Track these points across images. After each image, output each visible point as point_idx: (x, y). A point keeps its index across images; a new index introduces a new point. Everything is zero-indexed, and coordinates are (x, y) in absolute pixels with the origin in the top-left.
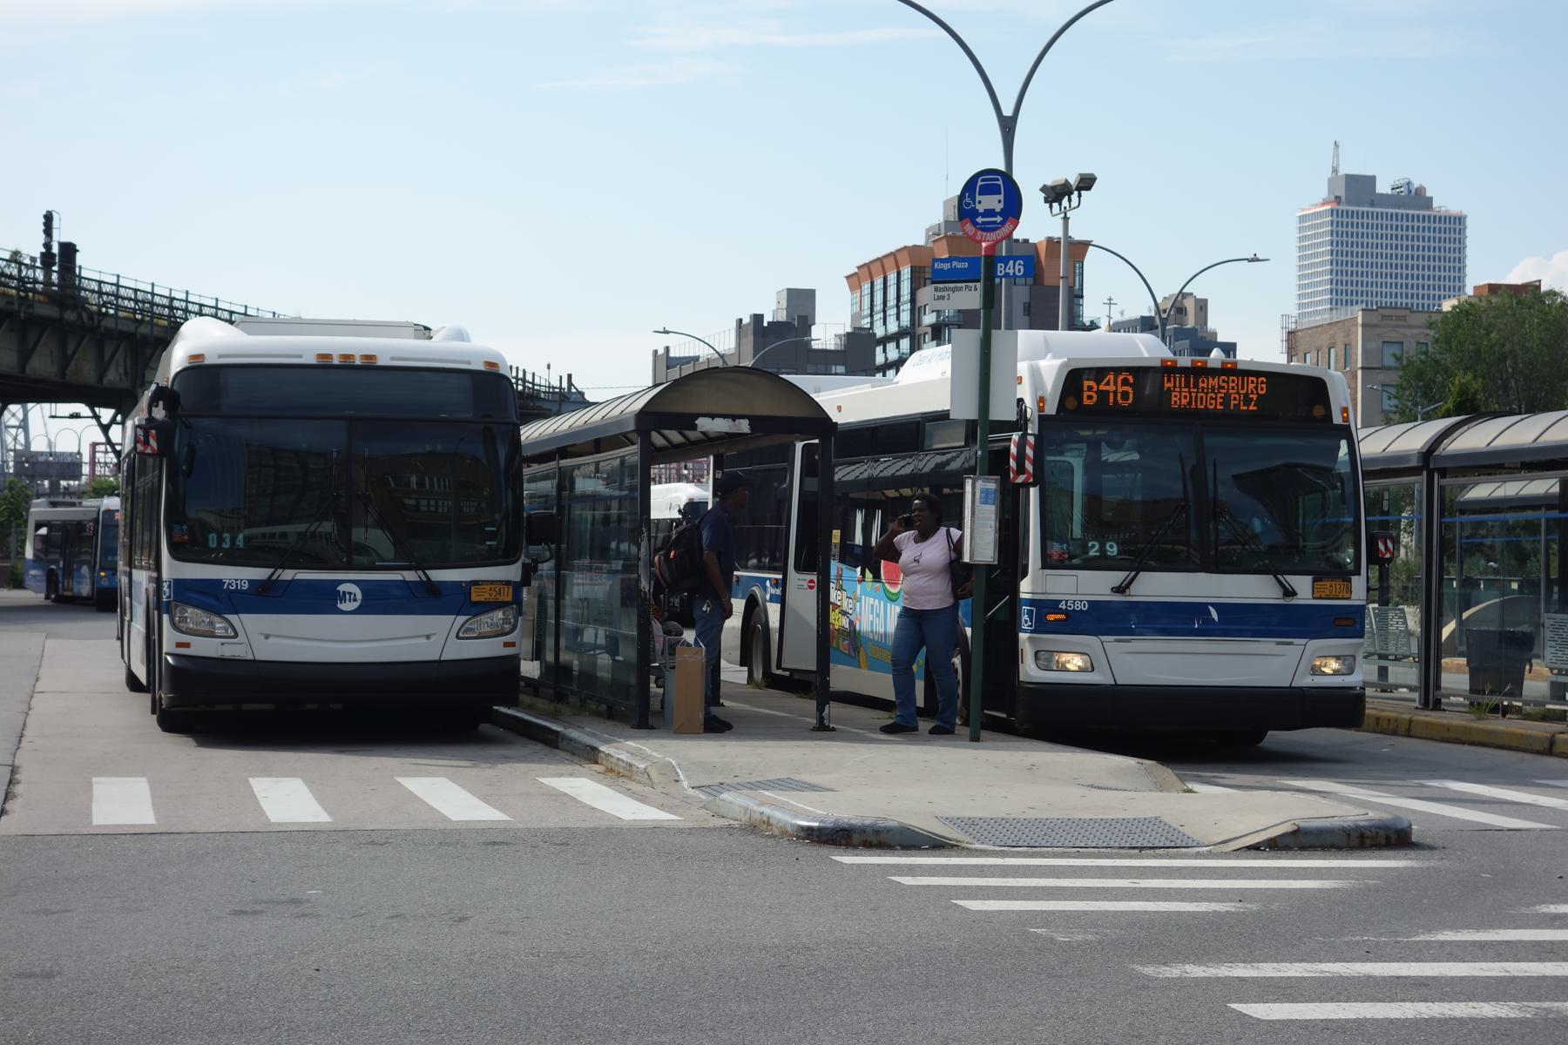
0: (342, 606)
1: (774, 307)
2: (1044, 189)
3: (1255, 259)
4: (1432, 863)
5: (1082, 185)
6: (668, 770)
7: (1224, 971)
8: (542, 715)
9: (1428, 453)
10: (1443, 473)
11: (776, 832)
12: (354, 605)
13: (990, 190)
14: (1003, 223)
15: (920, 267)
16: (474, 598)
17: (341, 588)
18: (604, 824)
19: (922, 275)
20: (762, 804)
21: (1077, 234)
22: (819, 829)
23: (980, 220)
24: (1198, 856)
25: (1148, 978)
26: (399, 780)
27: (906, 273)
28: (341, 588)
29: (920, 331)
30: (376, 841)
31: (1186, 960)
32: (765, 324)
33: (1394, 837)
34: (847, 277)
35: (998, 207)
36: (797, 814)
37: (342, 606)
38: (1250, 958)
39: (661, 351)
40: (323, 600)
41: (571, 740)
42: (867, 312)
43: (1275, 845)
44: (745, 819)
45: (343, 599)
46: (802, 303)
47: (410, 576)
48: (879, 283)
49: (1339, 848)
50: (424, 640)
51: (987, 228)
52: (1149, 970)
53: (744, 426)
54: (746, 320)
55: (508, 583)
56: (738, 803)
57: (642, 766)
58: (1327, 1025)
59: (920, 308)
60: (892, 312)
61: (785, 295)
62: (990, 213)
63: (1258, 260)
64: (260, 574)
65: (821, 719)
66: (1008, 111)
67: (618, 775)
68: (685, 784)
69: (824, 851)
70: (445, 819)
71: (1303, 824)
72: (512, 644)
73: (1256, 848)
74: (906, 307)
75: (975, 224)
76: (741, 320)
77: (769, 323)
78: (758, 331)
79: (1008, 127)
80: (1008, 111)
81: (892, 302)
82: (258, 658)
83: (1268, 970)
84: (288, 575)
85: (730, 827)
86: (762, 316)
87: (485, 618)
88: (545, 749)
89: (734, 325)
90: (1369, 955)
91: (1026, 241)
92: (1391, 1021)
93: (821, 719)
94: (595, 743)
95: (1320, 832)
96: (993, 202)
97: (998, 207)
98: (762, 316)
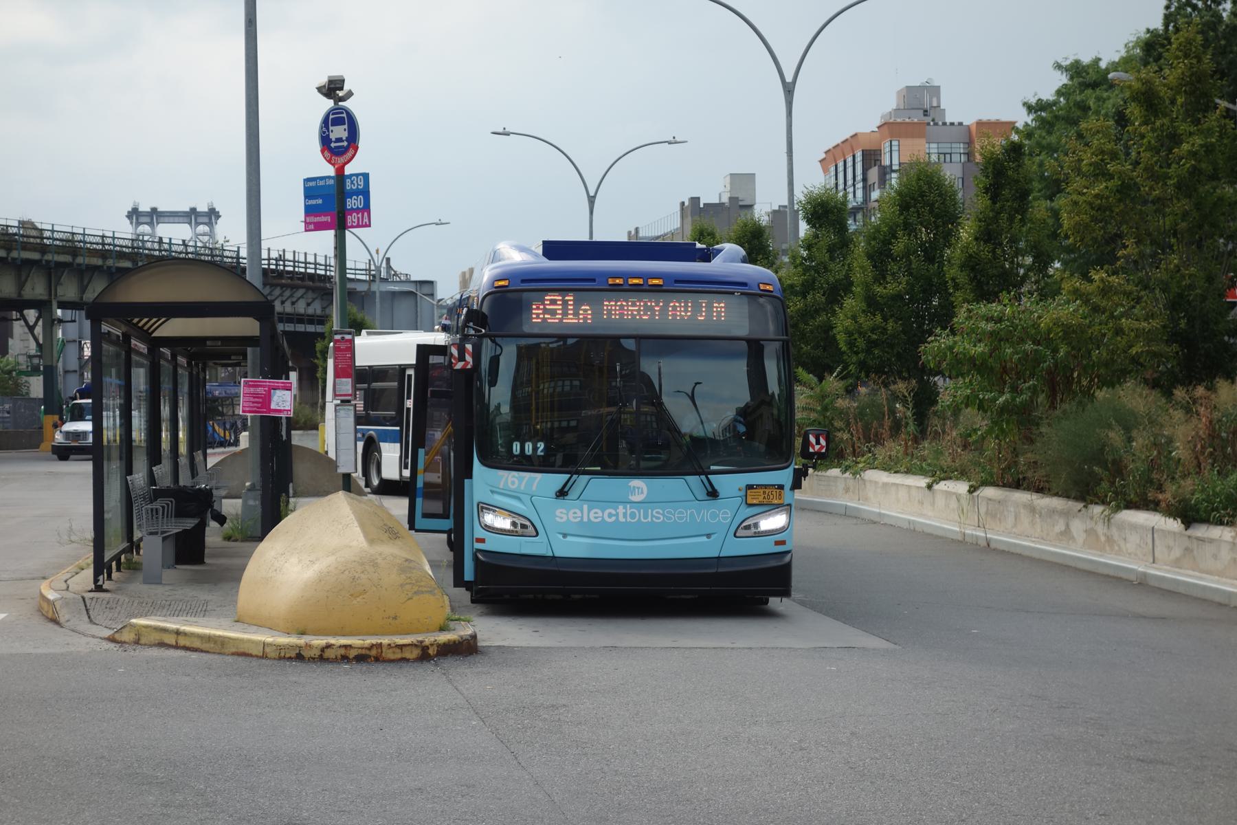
2: (320, 89)
5: (332, 86)
15: (874, 150)
19: (873, 157)
32: (702, 206)
34: (820, 161)
39: (633, 233)
48: (841, 168)
59: (870, 186)
60: (851, 190)
61: (728, 179)
63: (676, 143)
74: (860, 185)
76: (683, 203)
77: (704, 204)
81: (850, 182)
86: (699, 198)
89: (678, 208)
91: (960, 124)
98: (699, 198)
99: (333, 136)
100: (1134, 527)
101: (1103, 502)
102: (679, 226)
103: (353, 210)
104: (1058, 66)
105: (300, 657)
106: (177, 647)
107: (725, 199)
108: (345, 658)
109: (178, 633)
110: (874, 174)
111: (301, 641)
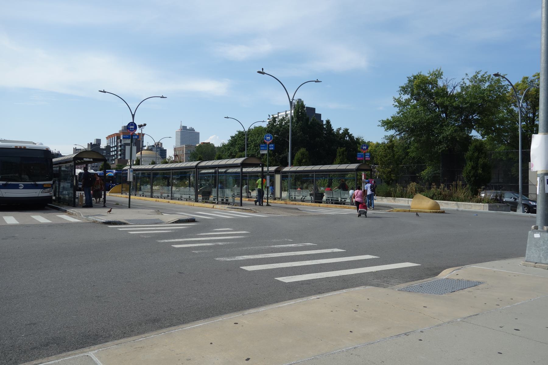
0: (20, 188)
1: (94, 141)
3: (170, 137)
4: (198, 224)
6: (79, 213)
7: (170, 241)
8: (57, 205)
9: (196, 166)
10: (198, 169)
11: (98, 222)
12: (22, 188)
13: (132, 125)
14: (134, 130)
16: (44, 186)
17: (20, 185)
18: (69, 222)
20: (96, 218)
21: (143, 133)
22: (105, 222)
23: (130, 129)
24: (165, 224)
25: (159, 242)
26: (31, 216)
27: (116, 137)
28: (20, 185)
29: (118, 146)
30: (28, 226)
31: (164, 239)
33: (192, 221)
34: (106, 137)
35: (133, 128)
36: (102, 220)
37: (20, 188)
38: (174, 239)
39: (75, 148)
40: (16, 187)
41: (62, 209)
42: (109, 143)
43: (176, 222)
44: (93, 221)
45: (20, 186)
46: (98, 141)
47: (33, 183)
48: (111, 139)
49: (185, 222)
50: (35, 193)
51: (131, 131)
52: (159, 241)
53: (92, 160)
54: (89, 143)
55: (50, 184)
56: (91, 218)
57: (75, 213)
58: (186, 247)
61: (96, 140)
62: (132, 129)
64: (4, 182)
65: (104, 205)
66: (133, 114)
67: (70, 214)
68: (82, 216)
69: (106, 225)
70: (40, 222)
71: (180, 219)
72: (51, 194)
73: (173, 223)
74: (116, 142)
75: (129, 130)
78: (91, 145)
79: (133, 116)
80: (133, 114)
82: (5, 196)
83: (177, 240)
84: (10, 183)
85: (90, 222)
87: (46, 190)
88: (57, 211)
90: (191, 237)
92: (195, 247)
93: (104, 205)
94: (66, 209)
95: (182, 220)
96: (133, 127)
97: (133, 128)
99: (363, 148)
100: (403, 200)
101: (391, 197)
102: (87, 147)
103: (366, 158)
104: (237, 131)
105: (436, 213)
106: (409, 212)
107: (95, 143)
108: (441, 213)
109: (409, 210)
110: (119, 141)
111: (436, 211)
